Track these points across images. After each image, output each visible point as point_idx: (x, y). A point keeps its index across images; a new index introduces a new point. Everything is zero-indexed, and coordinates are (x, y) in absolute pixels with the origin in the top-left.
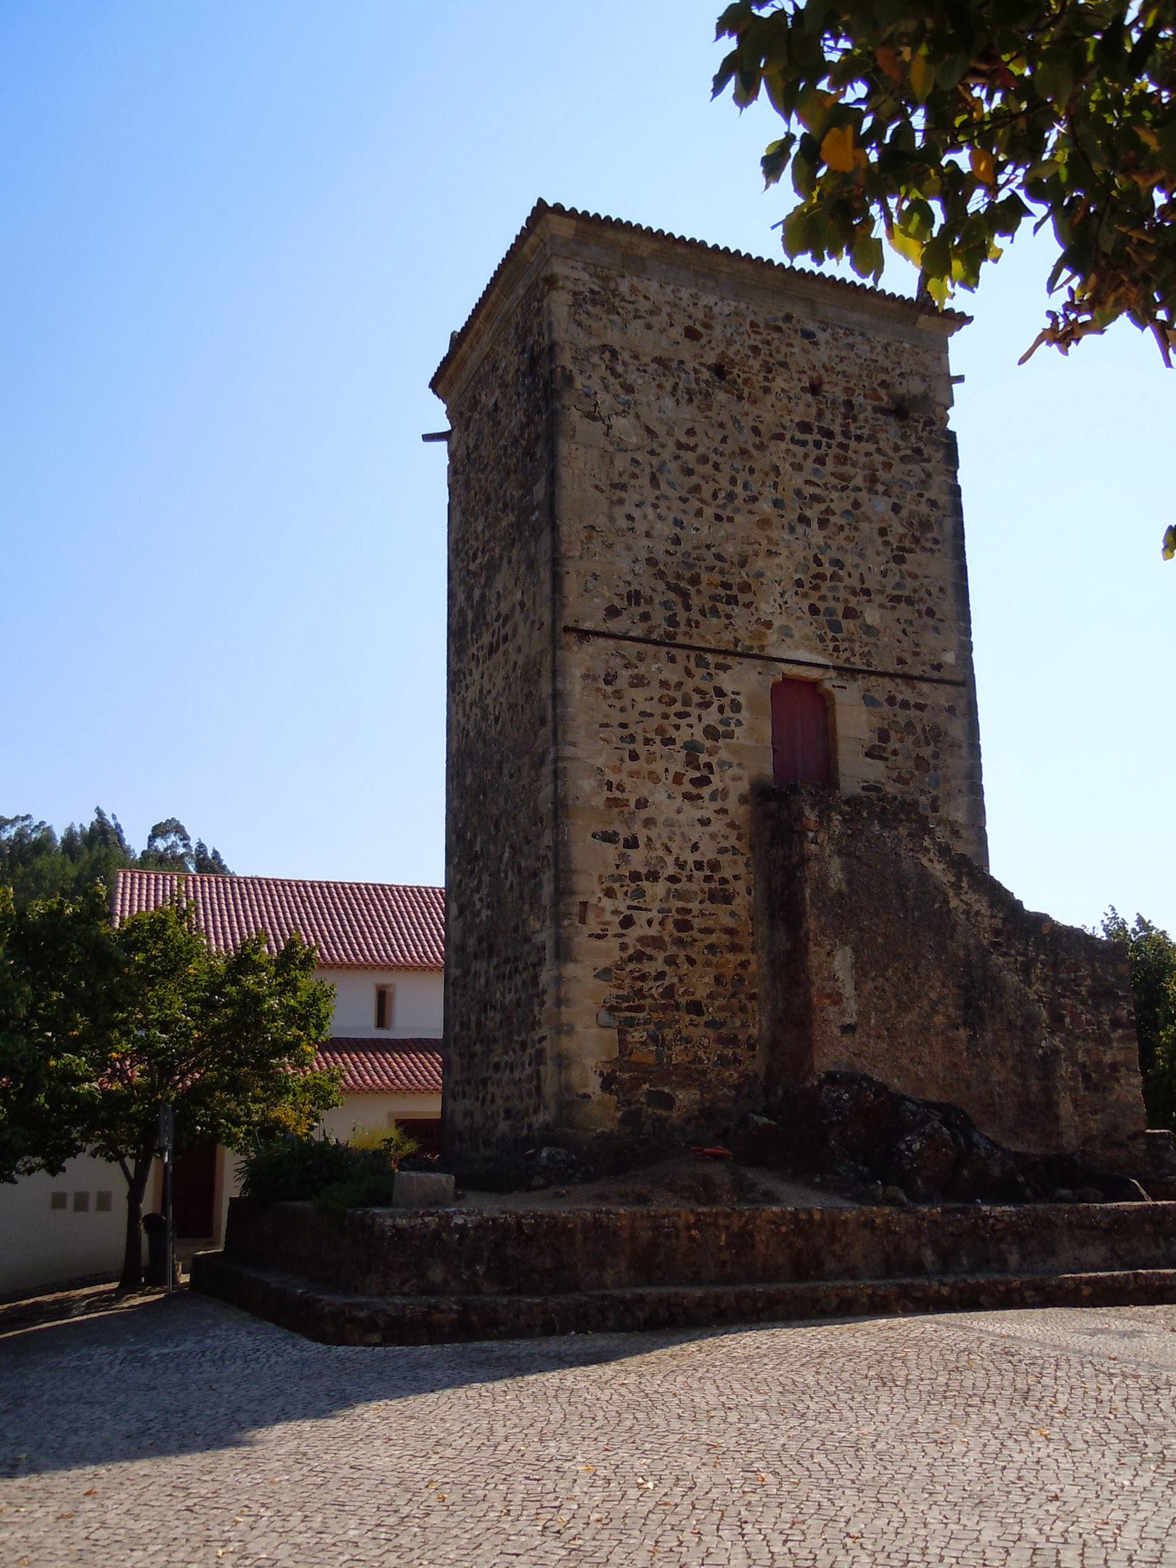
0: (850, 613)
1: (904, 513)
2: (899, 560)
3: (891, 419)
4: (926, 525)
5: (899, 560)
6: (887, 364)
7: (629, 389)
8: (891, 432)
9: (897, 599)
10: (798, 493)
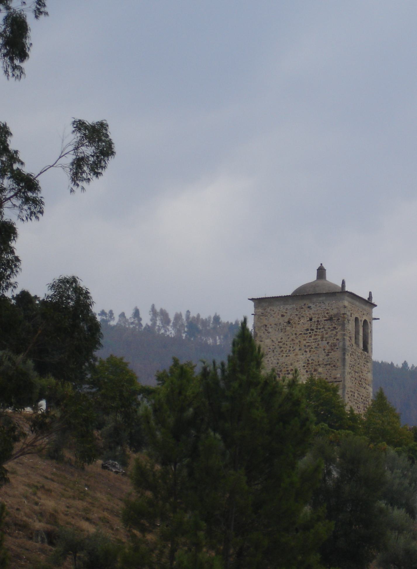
0: (315, 370)
1: (330, 344)
2: (328, 355)
3: (329, 322)
4: (335, 345)
5: (328, 355)
6: (329, 308)
7: (269, 333)
8: (328, 325)
9: (326, 365)
10: (305, 346)
